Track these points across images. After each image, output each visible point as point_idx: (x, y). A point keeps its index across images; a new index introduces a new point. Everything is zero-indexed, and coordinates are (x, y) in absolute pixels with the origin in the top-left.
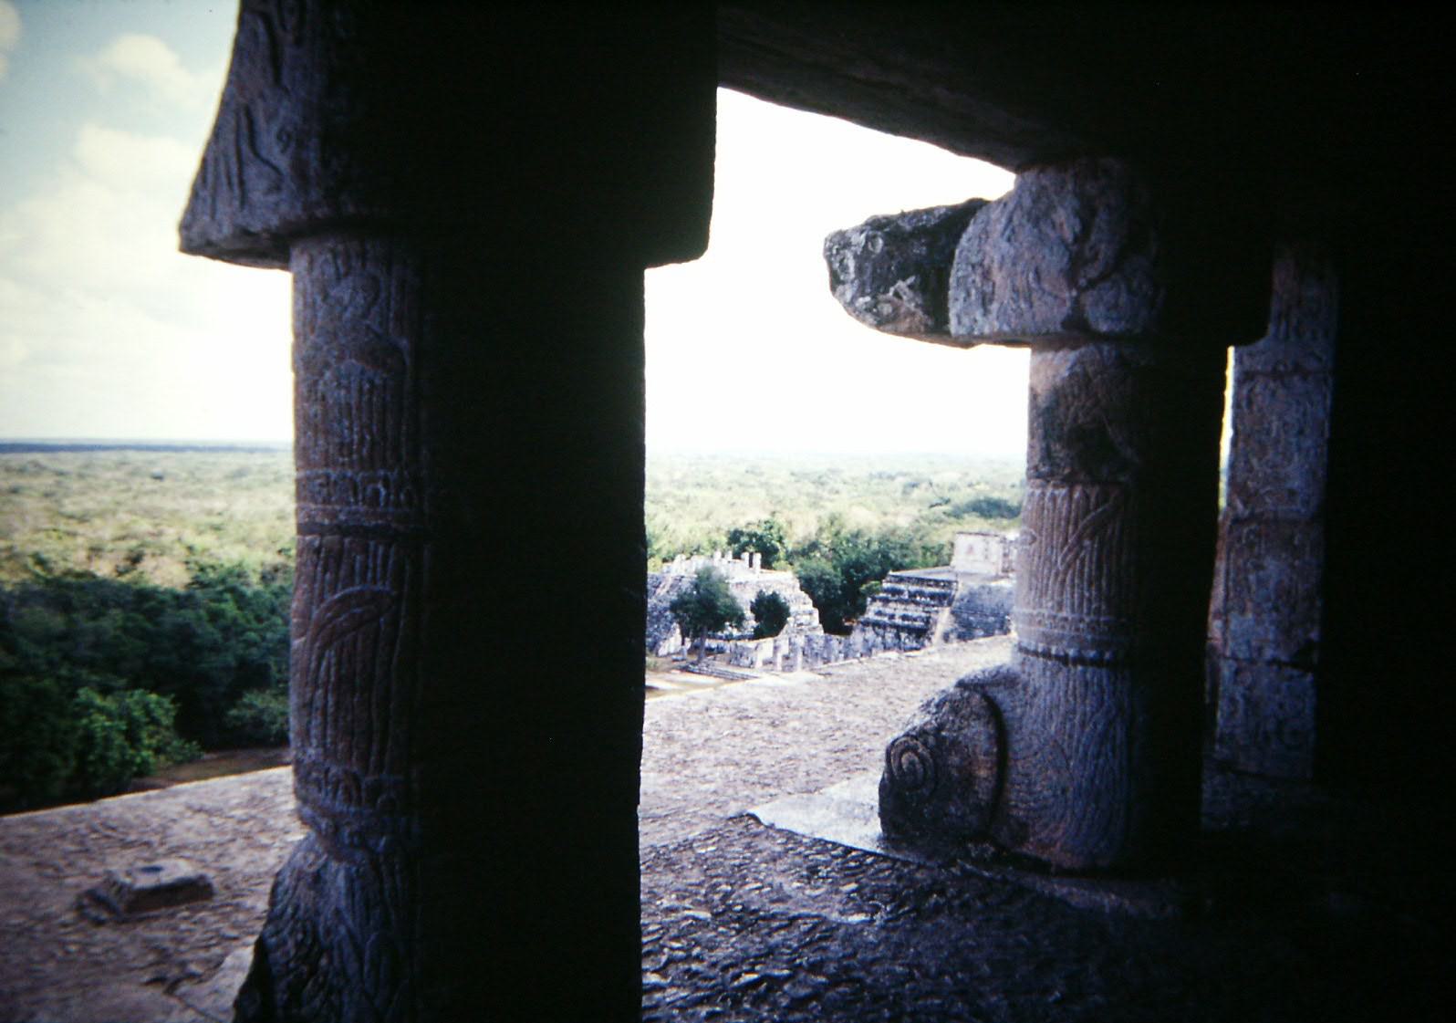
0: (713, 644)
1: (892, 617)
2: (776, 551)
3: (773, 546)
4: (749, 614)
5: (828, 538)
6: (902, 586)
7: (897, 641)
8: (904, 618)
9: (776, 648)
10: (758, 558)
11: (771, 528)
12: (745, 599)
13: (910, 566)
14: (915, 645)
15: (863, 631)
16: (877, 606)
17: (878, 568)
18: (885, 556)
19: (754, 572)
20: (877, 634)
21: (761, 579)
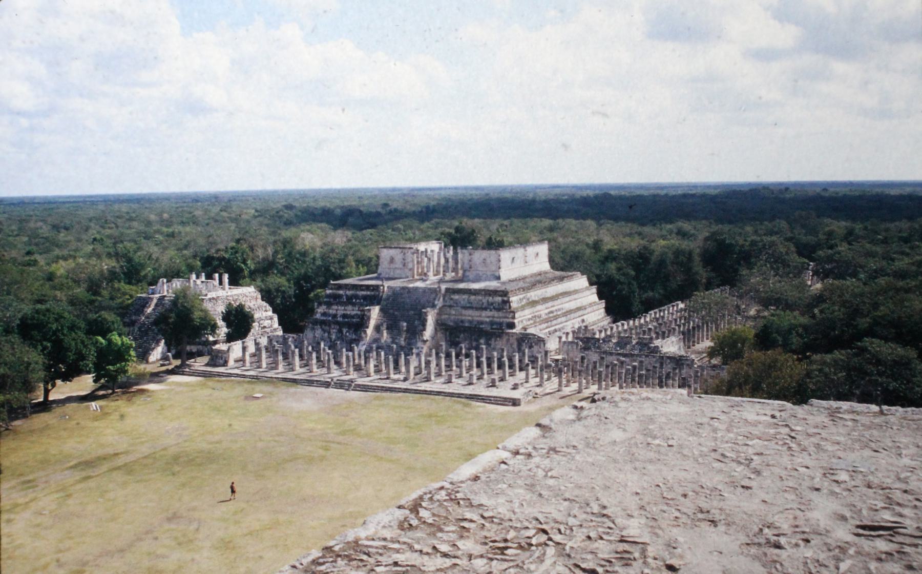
0: (194, 349)
1: (335, 316)
2: (242, 270)
3: (239, 267)
4: (221, 323)
5: (282, 258)
6: (341, 292)
8: (344, 316)
9: (244, 349)
10: (226, 277)
11: (236, 252)
12: (217, 311)
13: (347, 276)
14: (354, 337)
15: (313, 329)
16: (322, 309)
17: (321, 279)
18: (327, 269)
19: (224, 289)
20: (324, 331)
21: (229, 294)
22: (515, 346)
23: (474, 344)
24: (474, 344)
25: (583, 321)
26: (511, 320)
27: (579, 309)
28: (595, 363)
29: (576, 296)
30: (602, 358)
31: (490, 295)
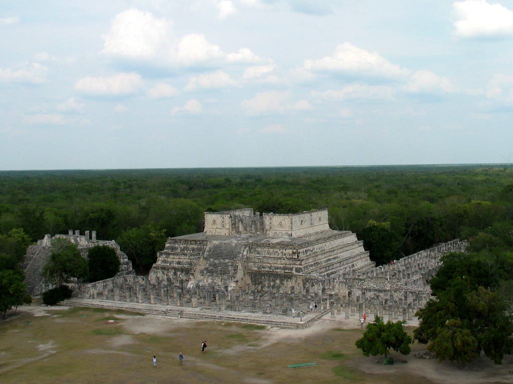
6: (177, 245)
7: (175, 277)
9: (105, 287)
10: (94, 234)
22: (301, 285)
23: (272, 284)
24: (272, 284)
25: (353, 266)
26: (299, 266)
27: (350, 258)
28: (358, 297)
29: (348, 248)
30: (364, 293)
31: (283, 248)
